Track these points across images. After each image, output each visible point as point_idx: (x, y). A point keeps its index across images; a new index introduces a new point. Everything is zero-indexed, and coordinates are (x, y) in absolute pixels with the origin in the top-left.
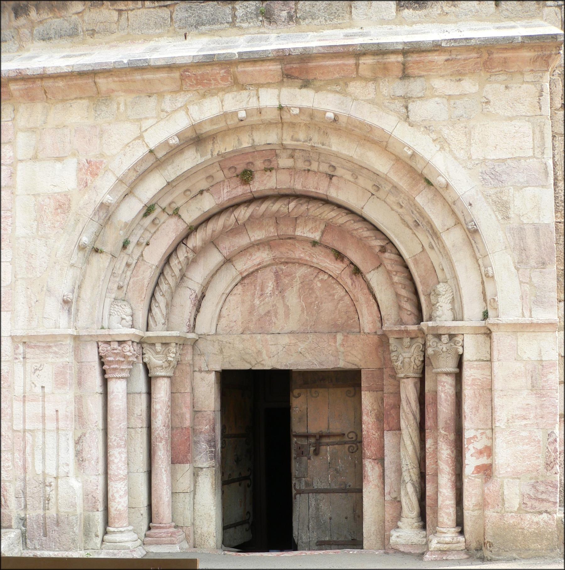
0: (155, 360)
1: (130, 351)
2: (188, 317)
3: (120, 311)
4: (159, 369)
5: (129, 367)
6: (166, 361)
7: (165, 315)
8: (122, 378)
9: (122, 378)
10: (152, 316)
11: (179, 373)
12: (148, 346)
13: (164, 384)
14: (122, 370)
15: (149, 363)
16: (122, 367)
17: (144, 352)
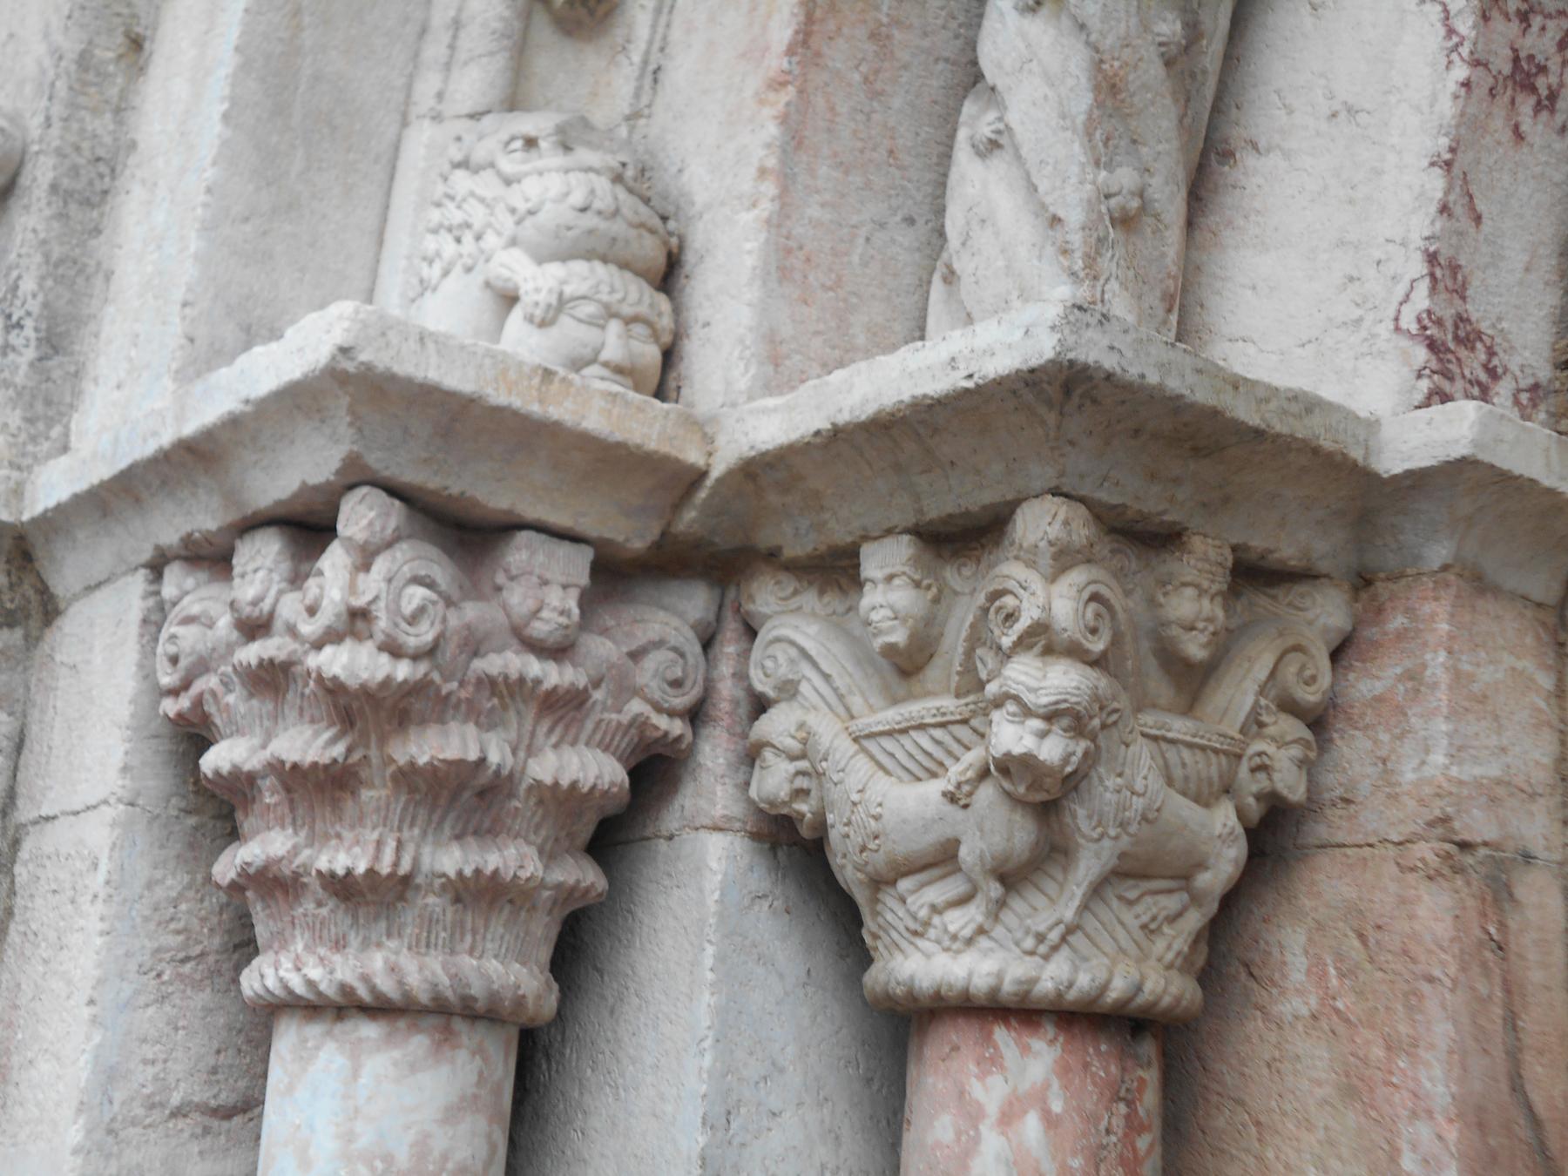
0: (862, 765)
1: (356, 621)
2: (1421, 225)
3: (478, 215)
4: (924, 895)
5: (451, 859)
6: (984, 774)
7: (1074, 216)
8: (380, 1009)
9: (380, 1009)
10: (951, 277)
11: (1317, 972)
12: (809, 599)
13: (1008, 1118)
14: (343, 888)
15: (821, 826)
16: (323, 864)
17: (762, 685)
